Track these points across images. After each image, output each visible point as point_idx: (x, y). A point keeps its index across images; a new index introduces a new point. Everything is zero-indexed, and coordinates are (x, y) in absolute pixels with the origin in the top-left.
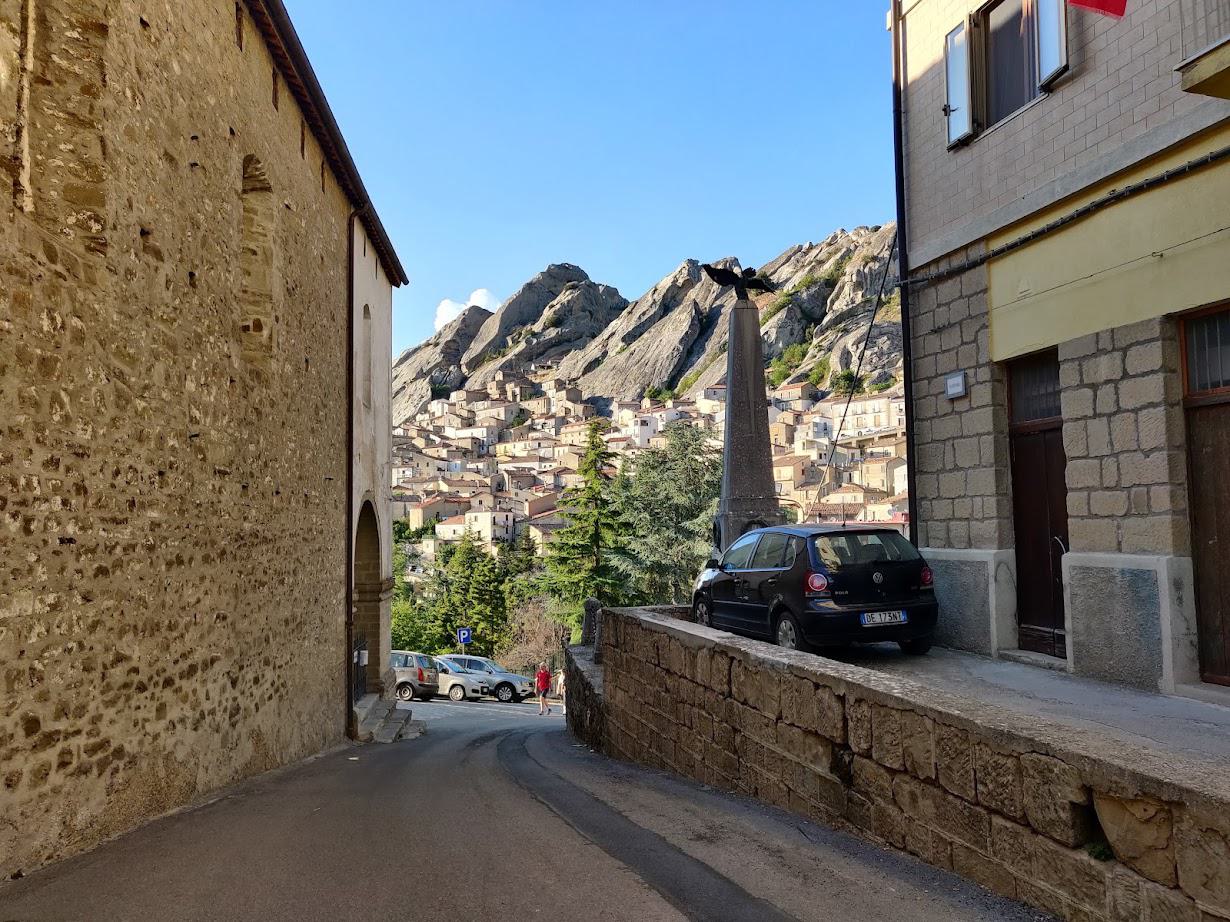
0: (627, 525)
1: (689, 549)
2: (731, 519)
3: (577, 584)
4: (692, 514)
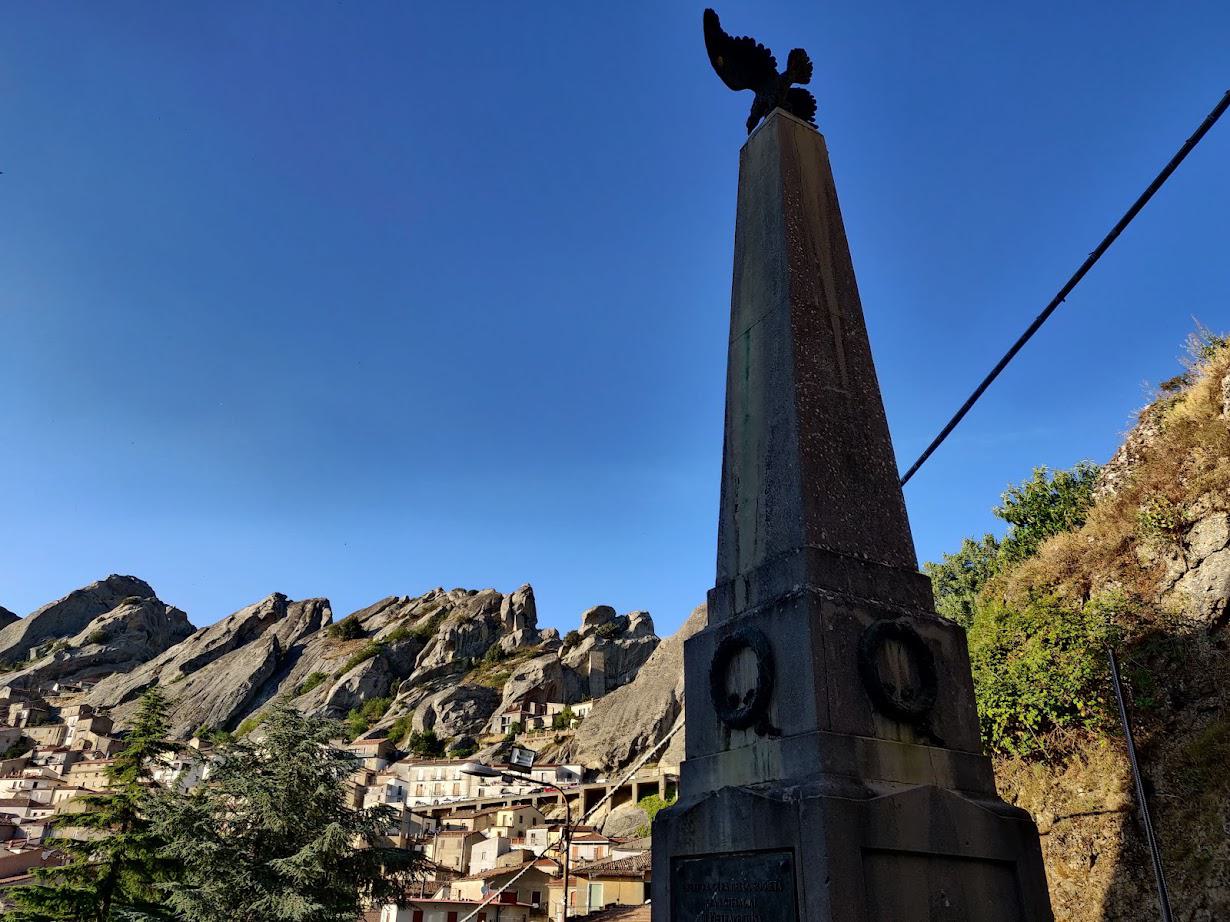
0: (174, 867)
1: (268, 908)
2: (828, 610)
4: (287, 844)
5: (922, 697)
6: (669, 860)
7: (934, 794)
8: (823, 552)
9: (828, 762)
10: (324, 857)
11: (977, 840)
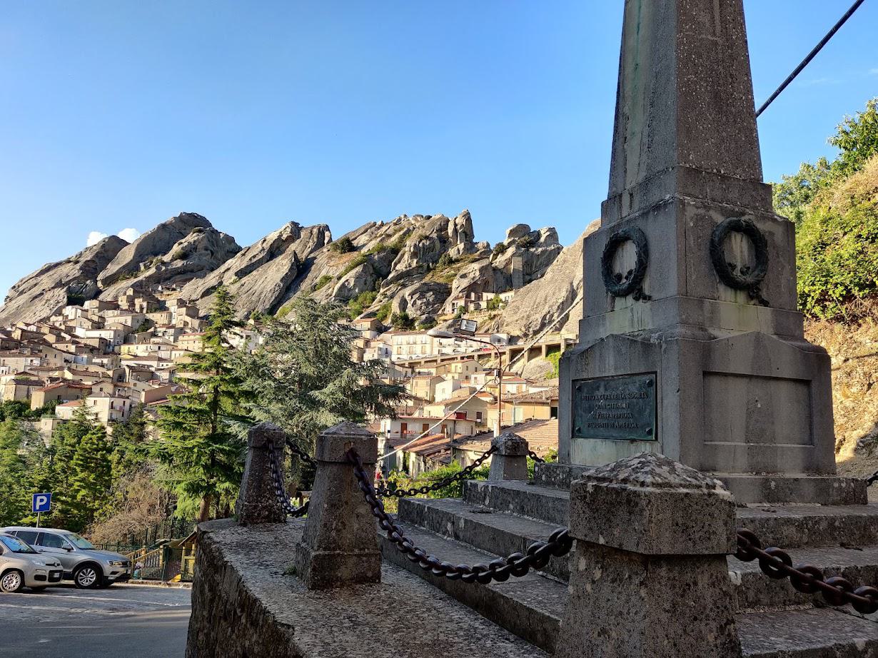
0: (250, 395)
1: (312, 419)
2: (691, 212)
3: (191, 449)
4: (320, 382)
5: (756, 273)
6: (571, 382)
7: (758, 339)
8: (689, 170)
9: (684, 317)
10: (344, 390)
11: (786, 366)
